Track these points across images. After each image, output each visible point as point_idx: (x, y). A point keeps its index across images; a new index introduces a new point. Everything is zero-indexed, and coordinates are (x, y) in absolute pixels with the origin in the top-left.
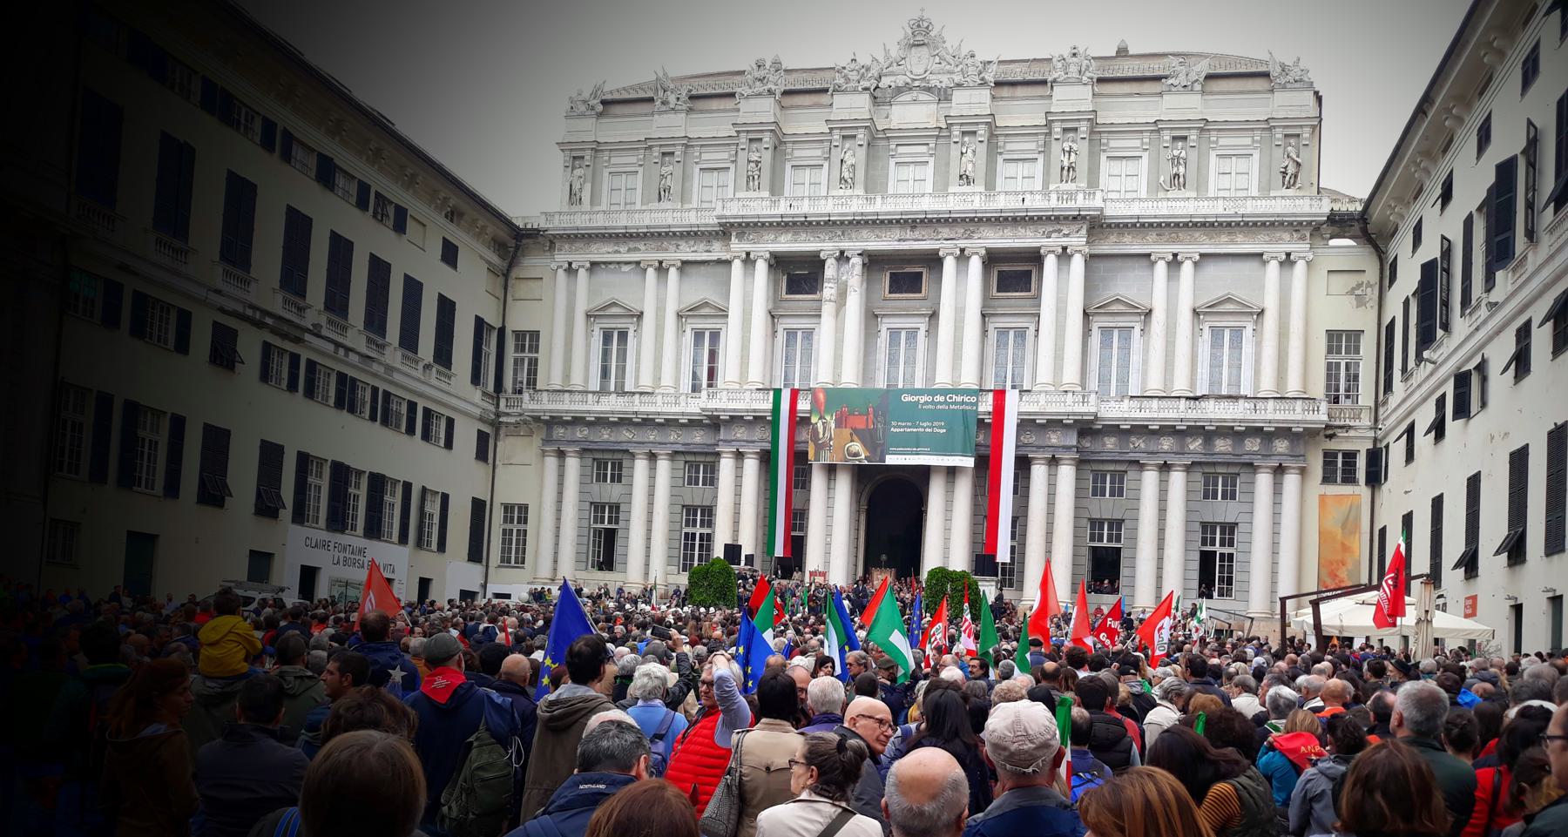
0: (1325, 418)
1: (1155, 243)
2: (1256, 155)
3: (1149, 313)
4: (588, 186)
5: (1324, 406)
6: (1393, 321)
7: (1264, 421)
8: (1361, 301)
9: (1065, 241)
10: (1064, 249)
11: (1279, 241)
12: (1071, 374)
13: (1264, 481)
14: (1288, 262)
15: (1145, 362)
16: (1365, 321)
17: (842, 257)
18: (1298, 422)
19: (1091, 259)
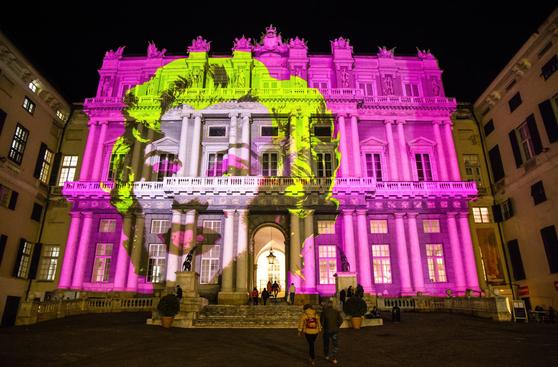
0: (476, 190)
1: (386, 115)
2: (421, 84)
3: (387, 146)
4: (111, 89)
5: (474, 185)
6: (497, 147)
7: (450, 192)
8: (474, 143)
9: (348, 111)
10: (348, 114)
11: (437, 116)
12: (358, 171)
13: (452, 222)
14: (442, 126)
15: (389, 168)
16: (478, 149)
17: (239, 116)
18: (465, 192)
19: (359, 121)
